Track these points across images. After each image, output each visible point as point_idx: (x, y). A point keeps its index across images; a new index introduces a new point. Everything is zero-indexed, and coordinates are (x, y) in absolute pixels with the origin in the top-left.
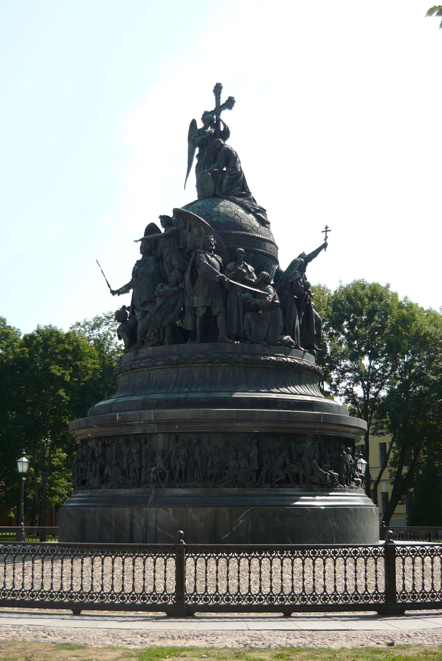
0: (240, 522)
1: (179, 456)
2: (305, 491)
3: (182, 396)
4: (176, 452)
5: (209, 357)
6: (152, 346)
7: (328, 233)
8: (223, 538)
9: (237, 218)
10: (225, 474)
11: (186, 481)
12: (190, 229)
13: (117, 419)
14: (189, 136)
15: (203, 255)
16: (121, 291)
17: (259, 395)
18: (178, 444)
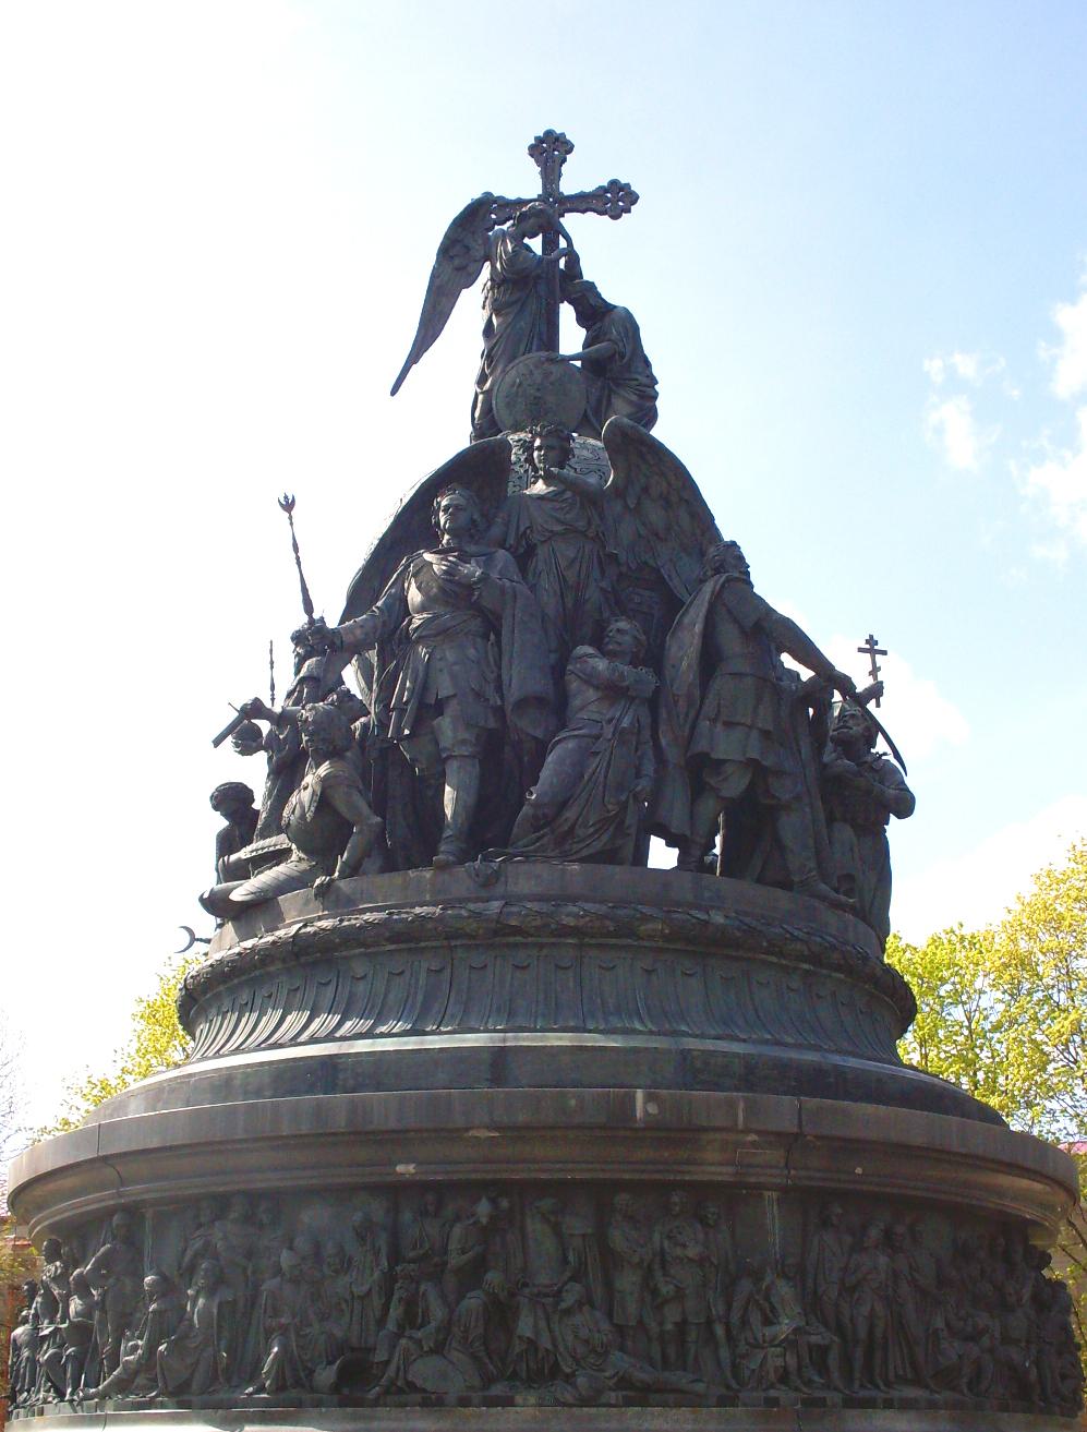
6: (581, 860)
7: (878, 657)
11: (888, 1384)
13: (639, 1113)
14: (446, 236)
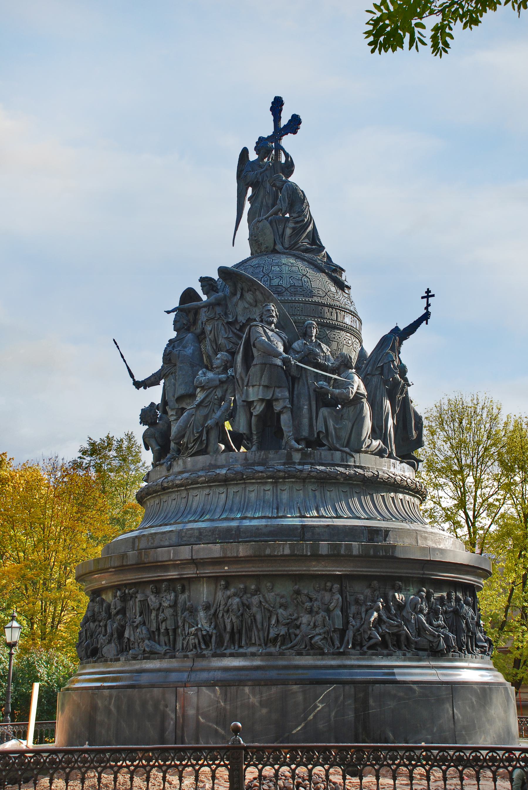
0: (319, 707)
1: (231, 610)
2: (410, 660)
3: (234, 524)
4: (226, 604)
5: (271, 469)
6: (191, 456)
8: (294, 732)
9: (305, 279)
10: (296, 635)
11: (240, 647)
12: (242, 295)
15: (260, 330)
16: (149, 382)
17: (341, 522)
18: (228, 593)
